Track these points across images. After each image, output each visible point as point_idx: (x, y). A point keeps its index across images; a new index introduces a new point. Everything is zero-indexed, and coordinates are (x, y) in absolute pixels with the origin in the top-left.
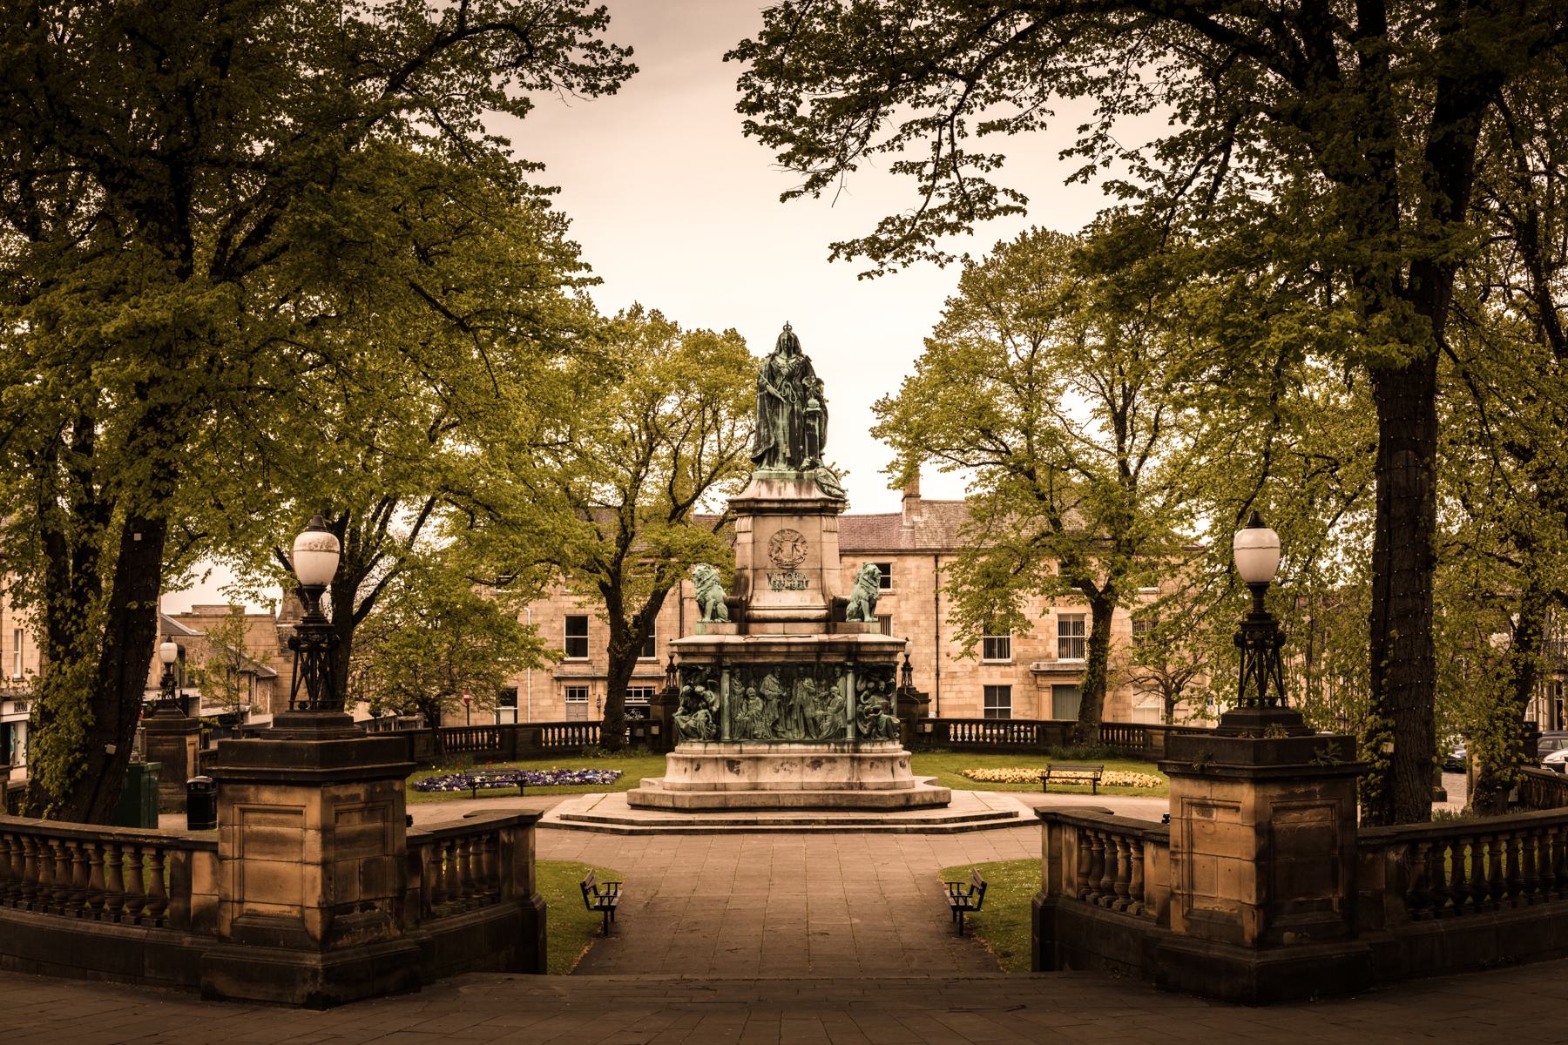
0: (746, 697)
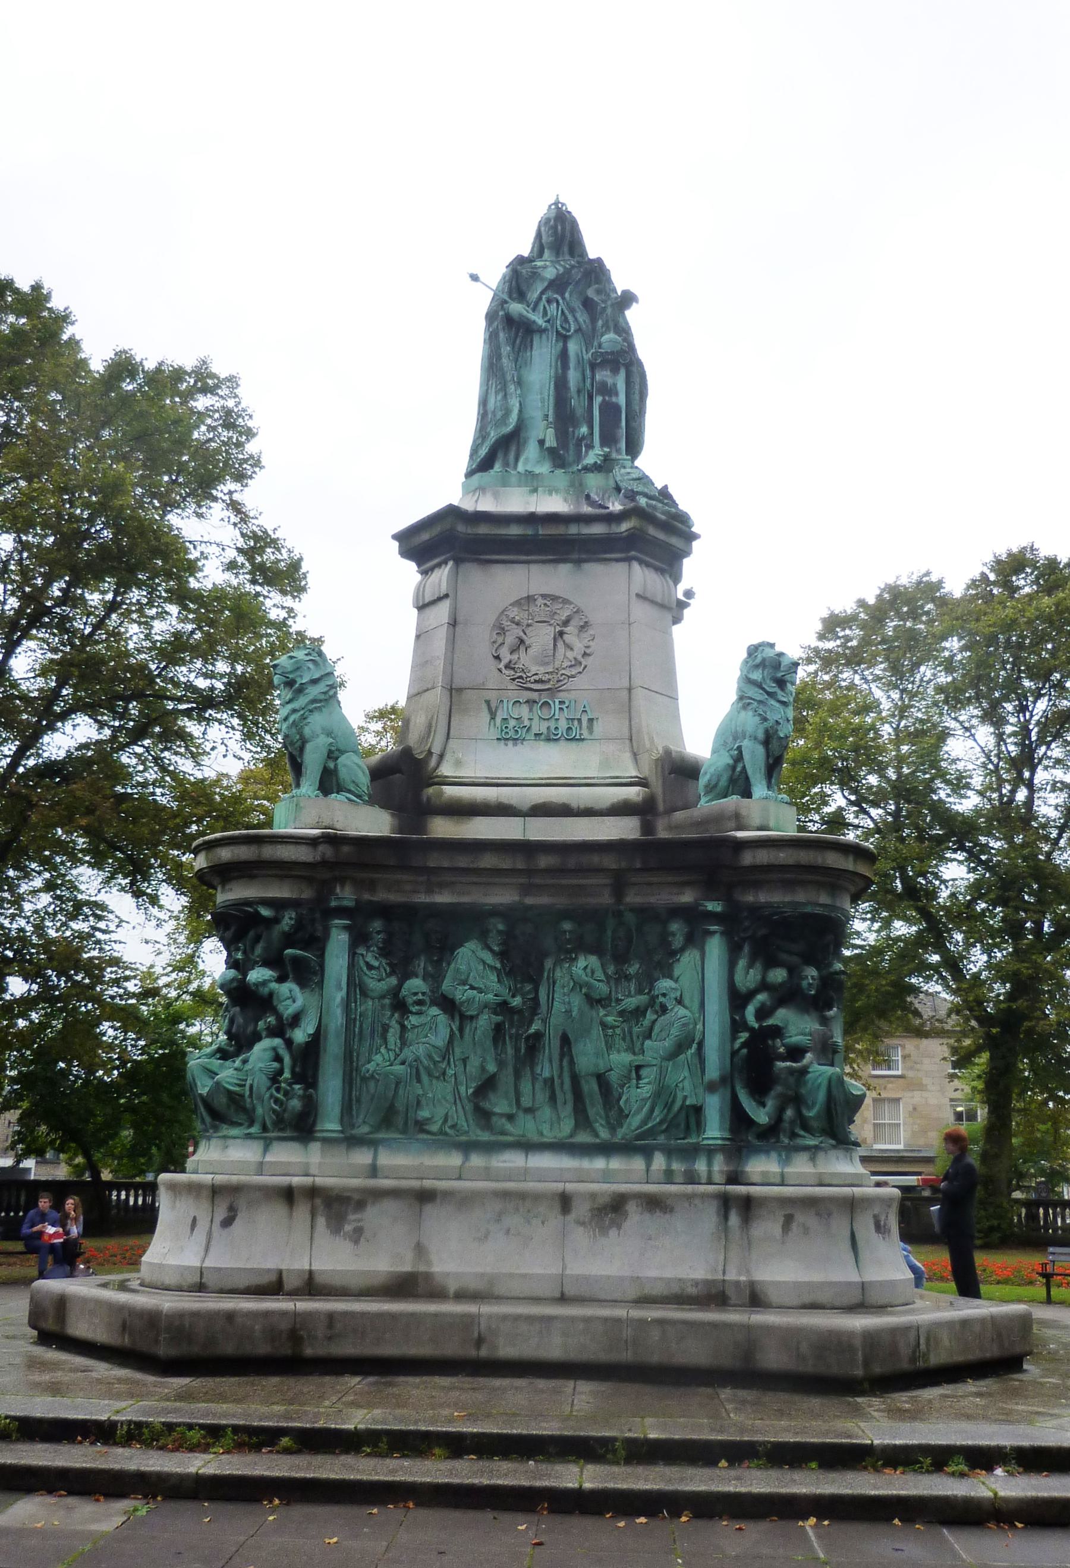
0: (400, 1006)
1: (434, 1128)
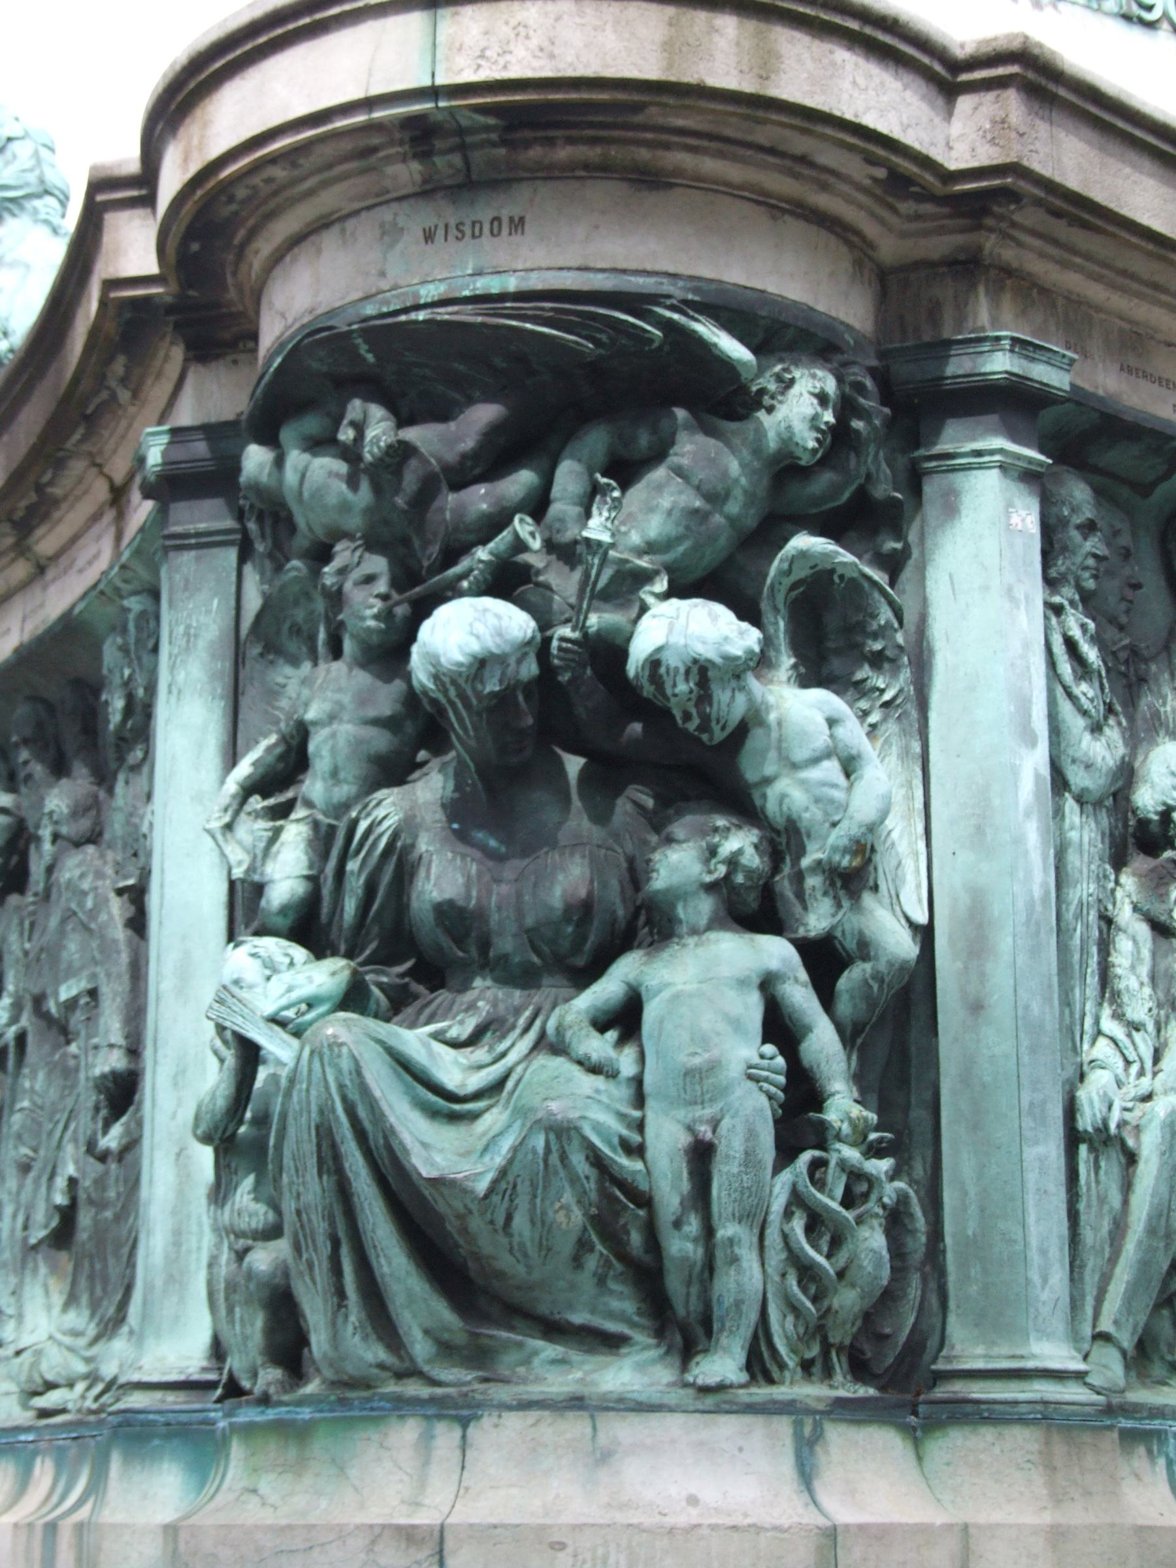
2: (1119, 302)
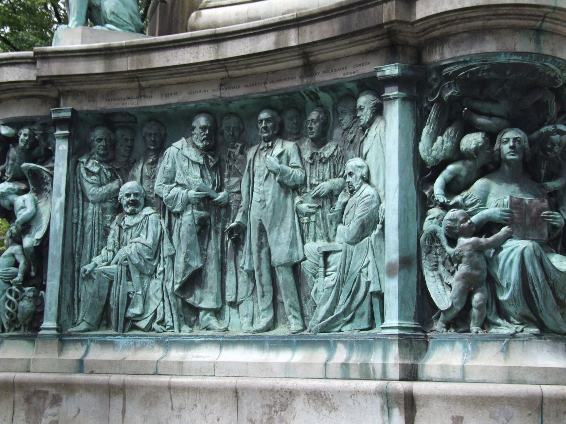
0: (118, 209)
1: (143, 324)
2: (102, 86)
